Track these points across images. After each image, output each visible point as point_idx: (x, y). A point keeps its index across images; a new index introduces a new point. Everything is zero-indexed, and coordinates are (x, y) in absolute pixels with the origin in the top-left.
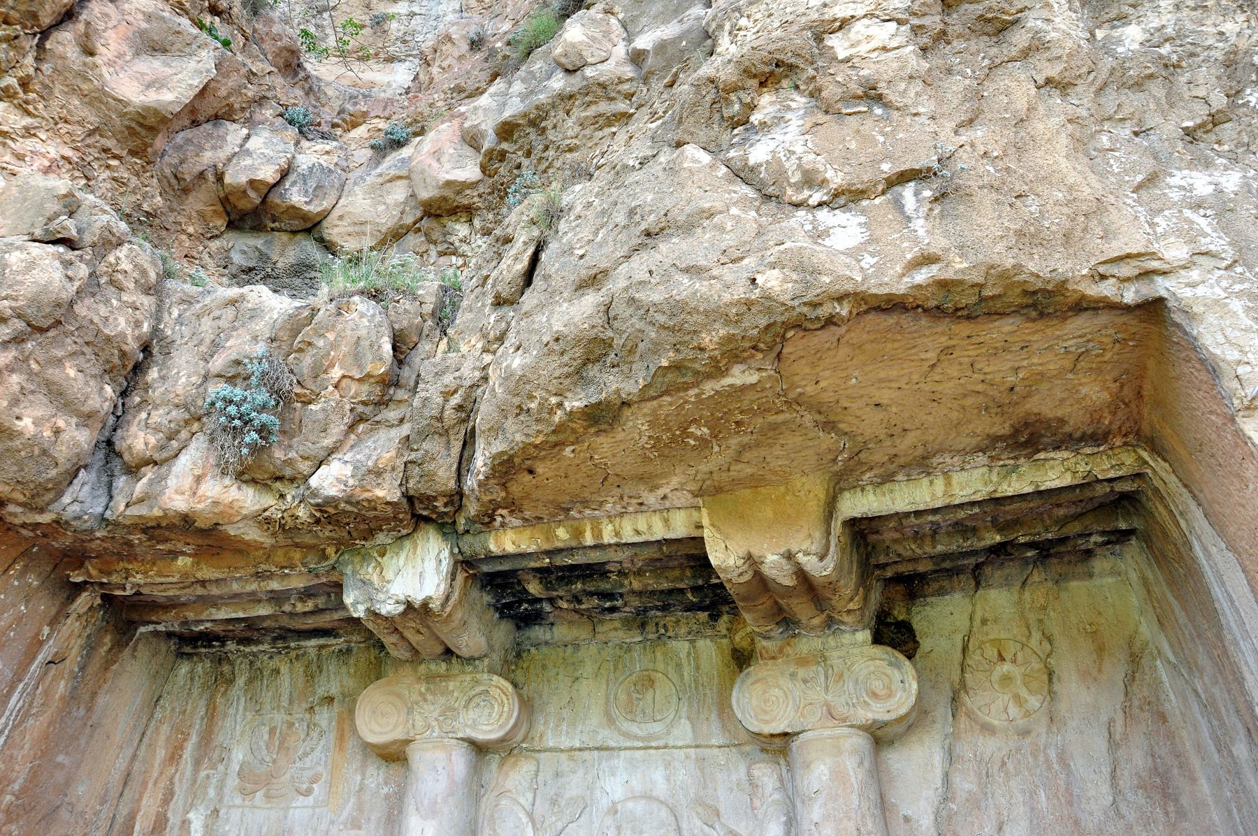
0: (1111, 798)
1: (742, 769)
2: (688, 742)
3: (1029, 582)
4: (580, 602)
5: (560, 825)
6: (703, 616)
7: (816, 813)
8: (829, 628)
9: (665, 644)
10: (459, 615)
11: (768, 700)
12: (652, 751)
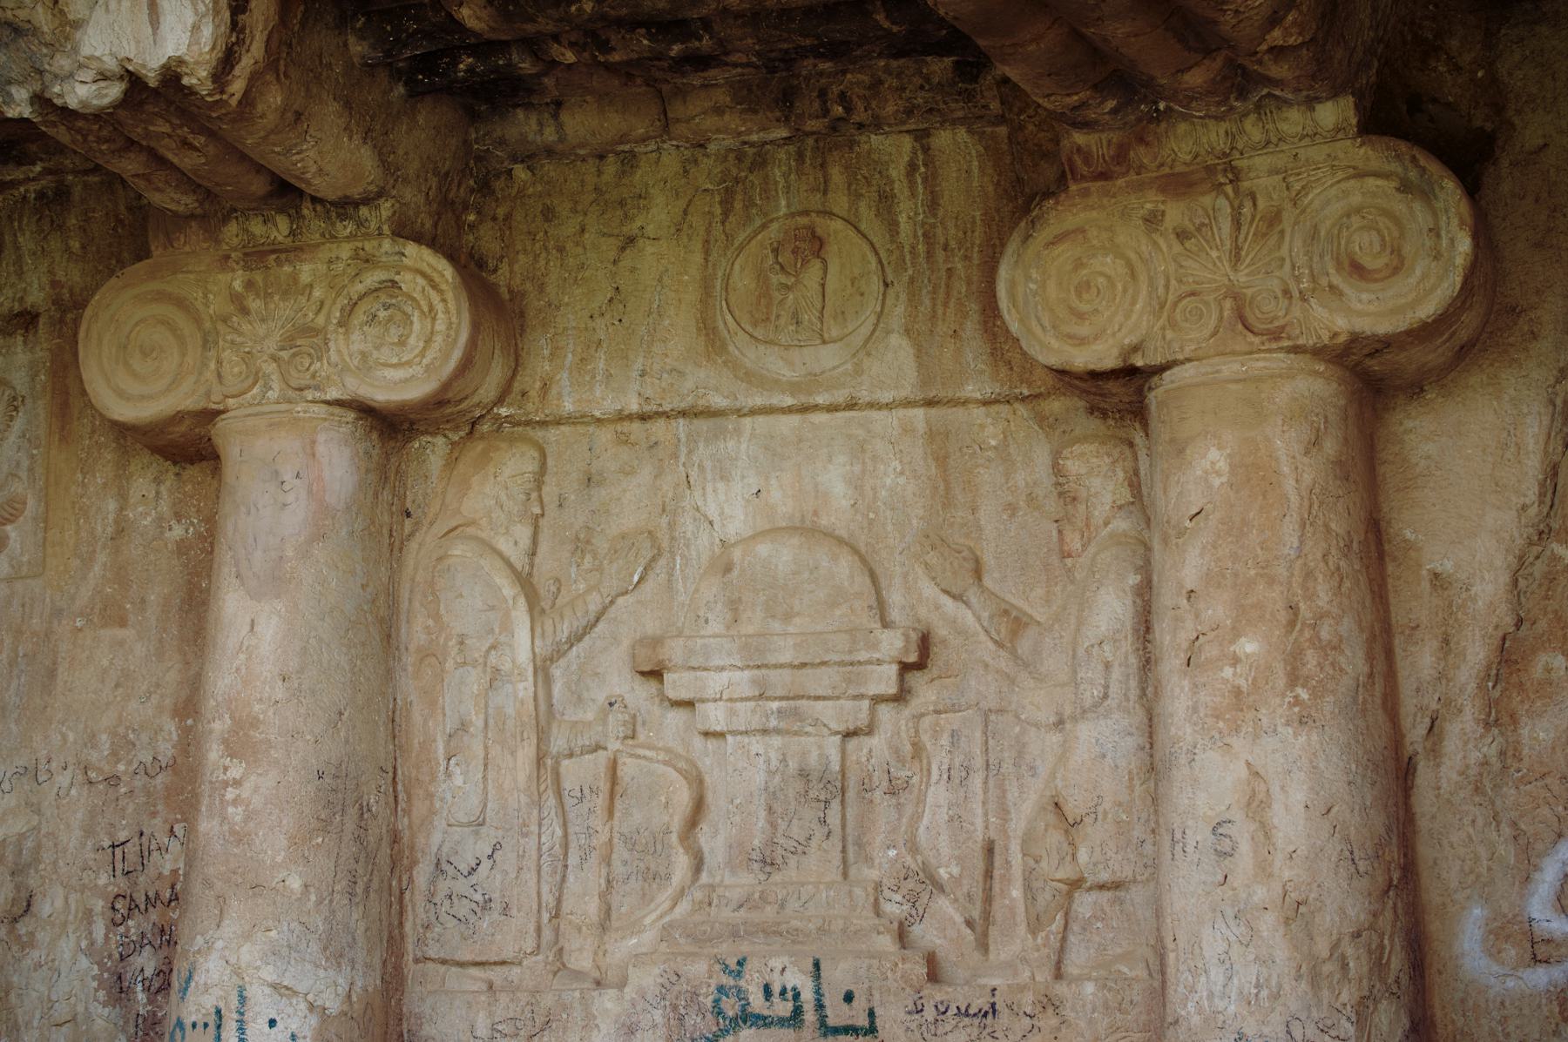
1: (1042, 456)
2: (906, 392)
4: (605, 47)
5: (594, 603)
7: (1188, 565)
8: (1242, 94)
9: (852, 144)
10: (273, 98)
11: (1094, 282)
12: (820, 418)
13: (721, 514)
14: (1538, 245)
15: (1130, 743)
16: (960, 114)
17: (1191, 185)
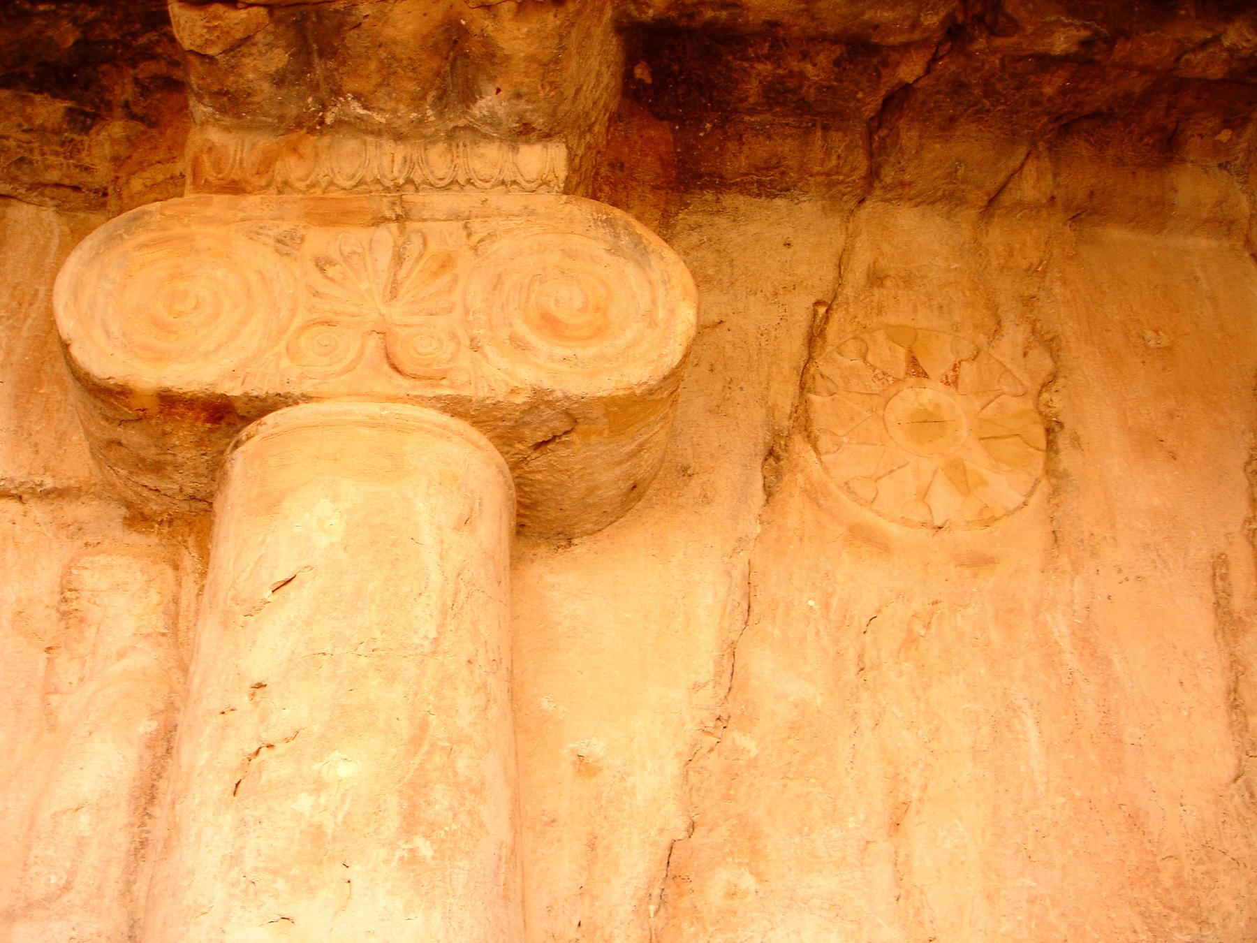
0: (1231, 761)
3: (1006, 199)
6: (48, 110)
7: (268, 647)
14: (715, 411)
16: (54, 176)
17: (346, 213)
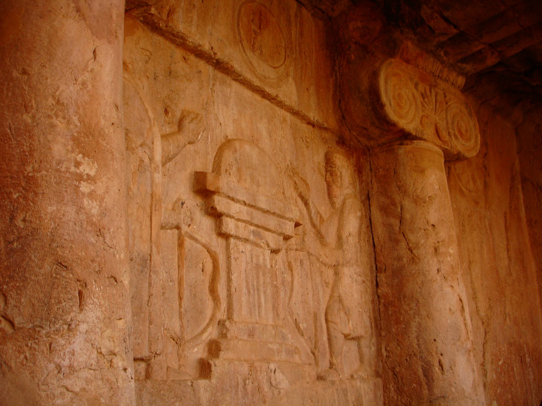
12: (258, 97)
13: (224, 122)
15: (360, 279)
